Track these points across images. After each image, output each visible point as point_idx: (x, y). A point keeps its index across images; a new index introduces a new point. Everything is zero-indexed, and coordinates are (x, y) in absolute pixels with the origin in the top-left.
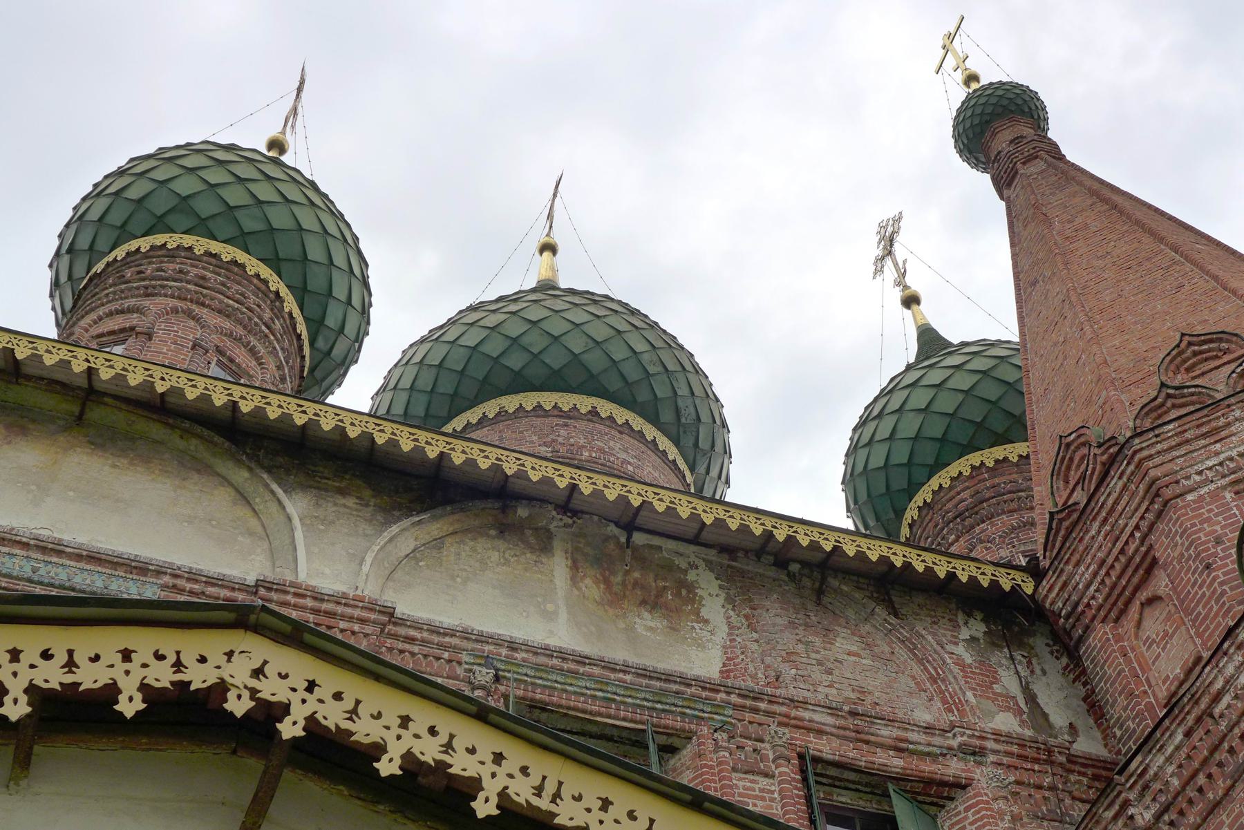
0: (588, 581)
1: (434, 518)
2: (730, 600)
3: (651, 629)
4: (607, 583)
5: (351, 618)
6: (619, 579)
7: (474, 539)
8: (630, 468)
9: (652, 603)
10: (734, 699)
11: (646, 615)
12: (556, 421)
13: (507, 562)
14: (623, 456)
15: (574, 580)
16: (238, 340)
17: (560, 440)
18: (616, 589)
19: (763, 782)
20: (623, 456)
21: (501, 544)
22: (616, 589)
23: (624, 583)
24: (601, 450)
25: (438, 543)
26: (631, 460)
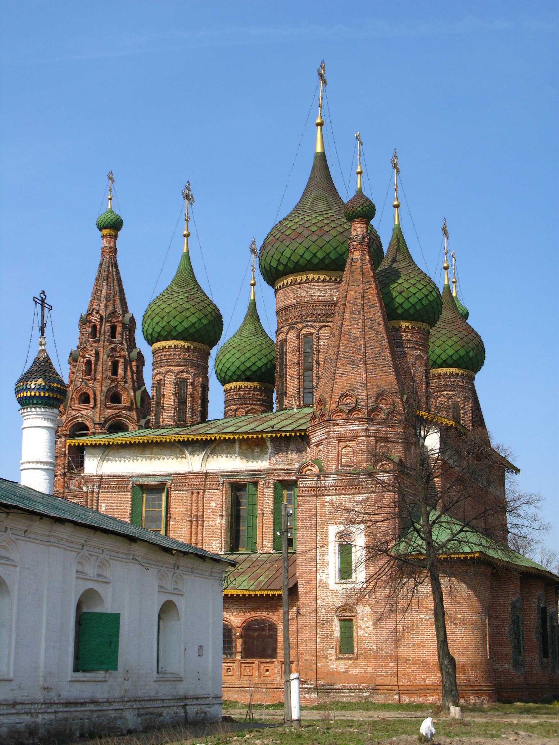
0: (243, 446)
1: (212, 444)
2: (271, 441)
3: (257, 452)
4: (248, 444)
5: (200, 476)
6: (250, 442)
7: (221, 444)
8: (320, 298)
9: (257, 445)
10: (265, 472)
11: (256, 448)
12: (297, 286)
13: (227, 449)
14: (319, 293)
15: (240, 448)
16: (182, 372)
17: (299, 295)
18: (250, 444)
19: (269, 489)
20: (319, 293)
21: (226, 444)
22: (250, 444)
23: (251, 442)
24: (311, 296)
25: (214, 449)
26: (321, 294)
